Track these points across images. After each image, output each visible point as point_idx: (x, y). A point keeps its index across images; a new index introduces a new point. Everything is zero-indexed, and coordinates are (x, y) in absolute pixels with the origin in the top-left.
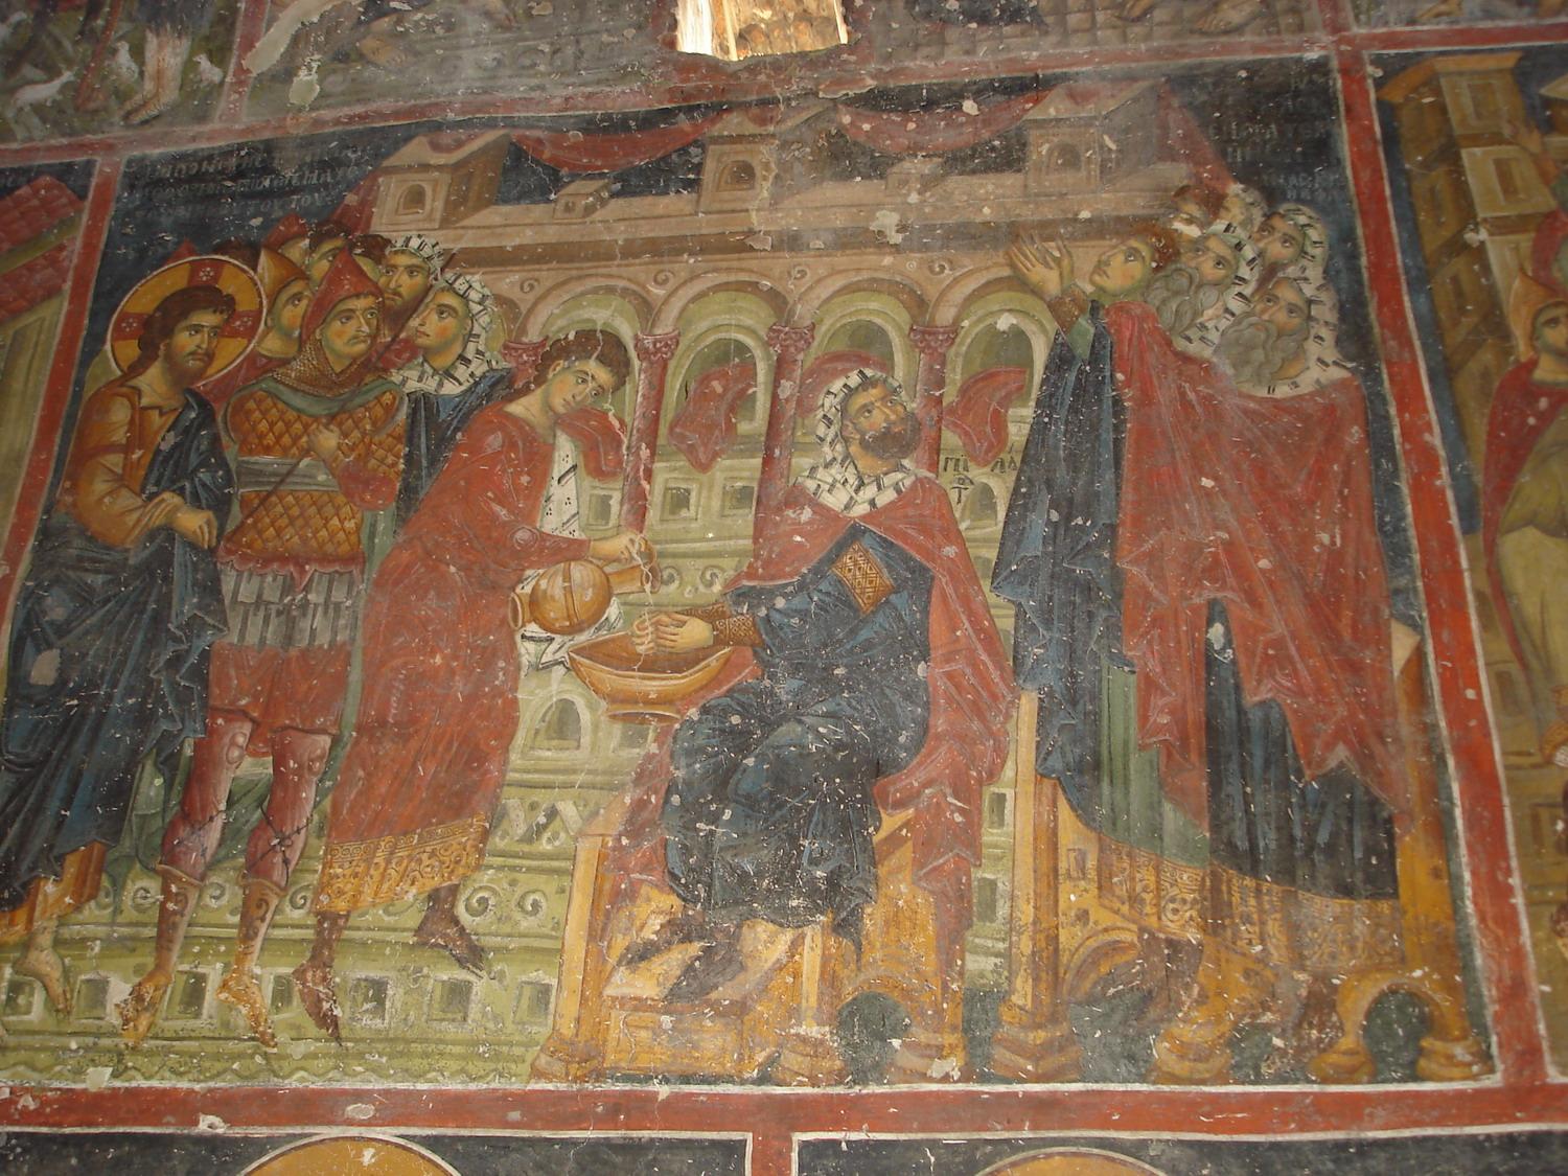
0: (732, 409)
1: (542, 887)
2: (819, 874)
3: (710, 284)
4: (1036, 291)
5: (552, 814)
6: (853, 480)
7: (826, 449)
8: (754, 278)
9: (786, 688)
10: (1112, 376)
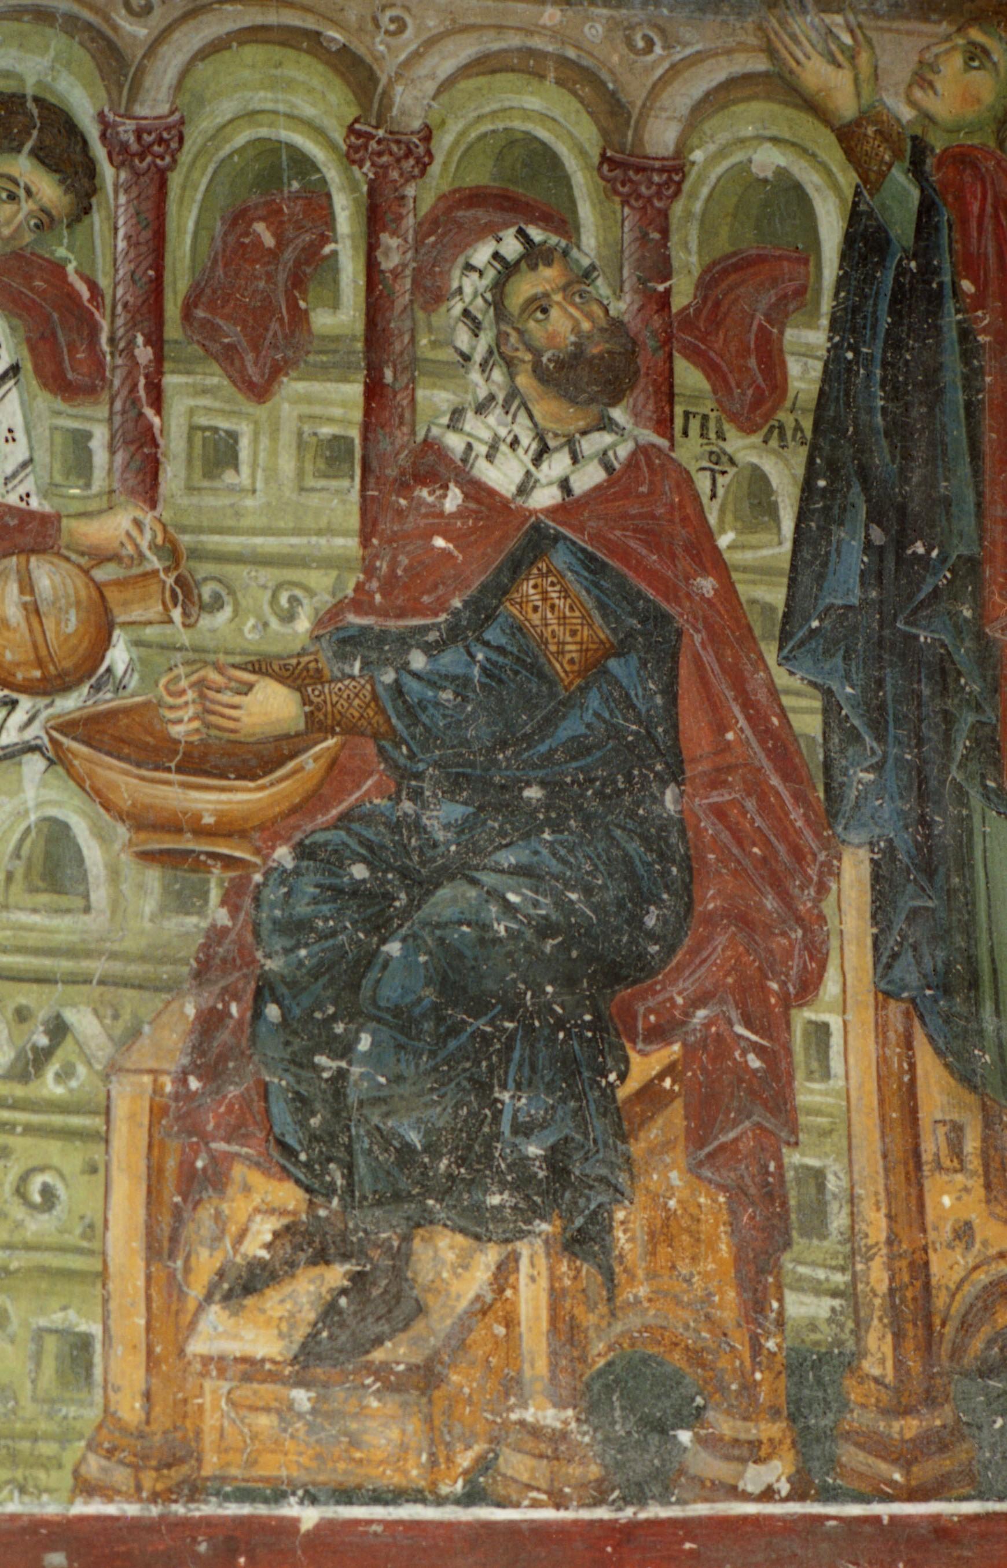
0: (297, 282)
1: (56, 1161)
2: (533, 1150)
3: (230, 26)
4: (813, 106)
5: (59, 1029)
6: (526, 439)
7: (475, 376)
8: (310, 23)
9: (442, 816)
10: (954, 284)
